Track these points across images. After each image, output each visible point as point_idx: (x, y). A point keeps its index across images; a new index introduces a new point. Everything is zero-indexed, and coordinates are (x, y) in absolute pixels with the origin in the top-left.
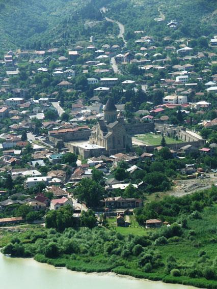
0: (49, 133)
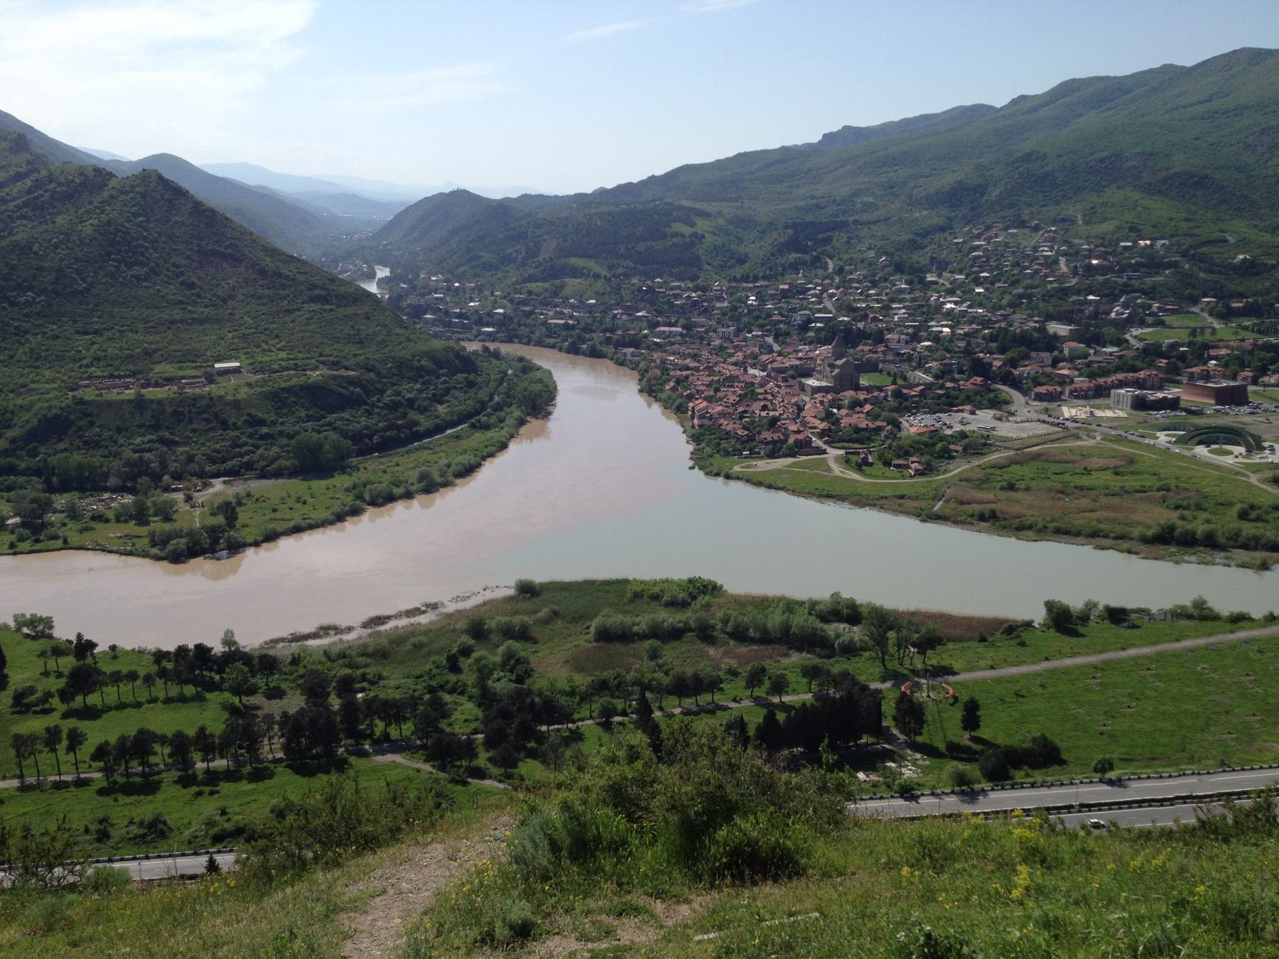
0: (769, 366)
